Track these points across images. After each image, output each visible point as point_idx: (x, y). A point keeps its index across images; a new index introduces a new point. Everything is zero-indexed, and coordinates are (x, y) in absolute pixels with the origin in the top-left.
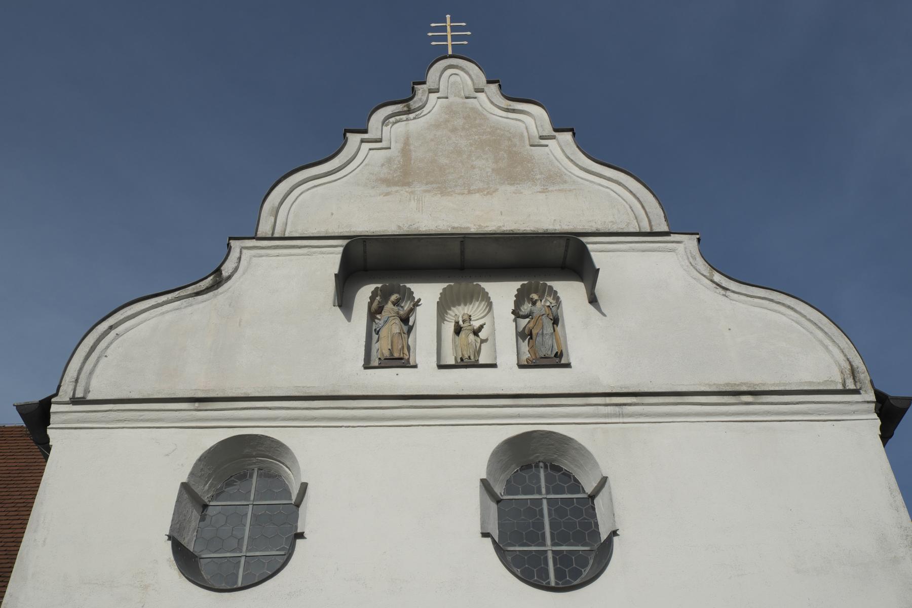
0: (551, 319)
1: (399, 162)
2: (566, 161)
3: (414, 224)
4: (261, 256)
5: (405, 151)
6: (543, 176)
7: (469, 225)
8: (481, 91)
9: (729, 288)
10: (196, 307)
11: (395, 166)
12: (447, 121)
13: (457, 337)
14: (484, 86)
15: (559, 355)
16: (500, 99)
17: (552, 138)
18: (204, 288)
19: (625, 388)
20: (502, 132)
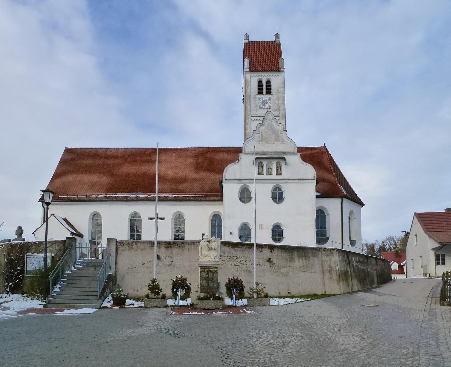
5: (262, 134)
12: (268, 127)
17: (283, 132)
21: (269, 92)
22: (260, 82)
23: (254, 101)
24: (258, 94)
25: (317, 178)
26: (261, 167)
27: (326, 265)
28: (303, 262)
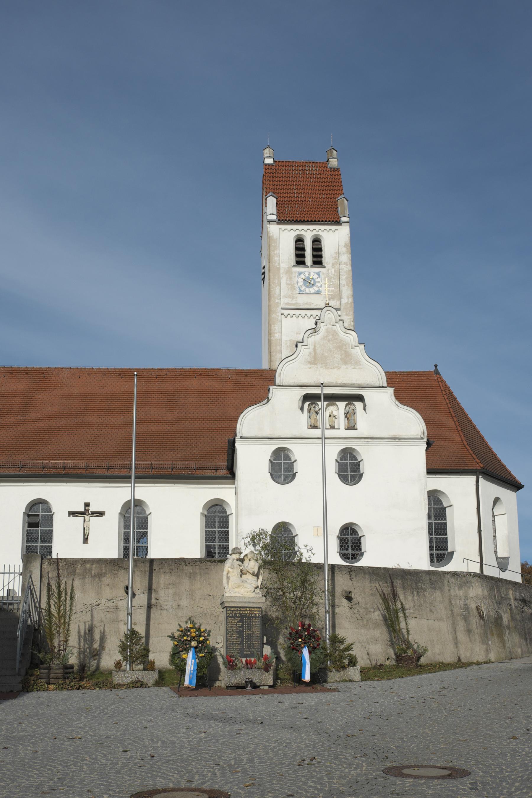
5: (315, 350)
12: (327, 336)
21: (318, 261)
22: (299, 240)
23: (287, 278)
24: (295, 264)
25: (427, 436)
26: (315, 414)
27: (459, 604)
28: (413, 600)
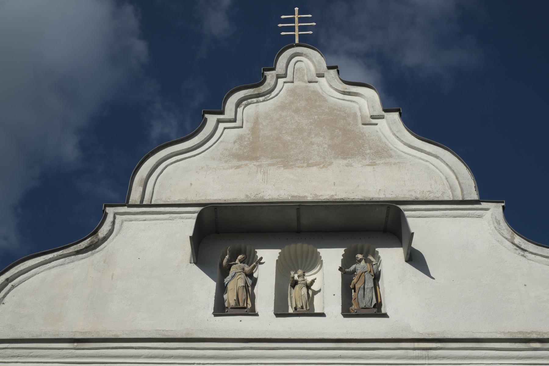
0: (372, 276)
1: (249, 139)
2: (393, 137)
3: (259, 194)
4: (132, 221)
5: (254, 130)
6: (372, 151)
7: (306, 194)
8: (321, 76)
9: (528, 249)
10: (76, 263)
11: (246, 143)
12: (291, 103)
13: (292, 289)
14: (325, 71)
15: (379, 305)
16: (338, 83)
17: (382, 117)
18: (83, 248)
19: (432, 334)
20: (338, 112)
